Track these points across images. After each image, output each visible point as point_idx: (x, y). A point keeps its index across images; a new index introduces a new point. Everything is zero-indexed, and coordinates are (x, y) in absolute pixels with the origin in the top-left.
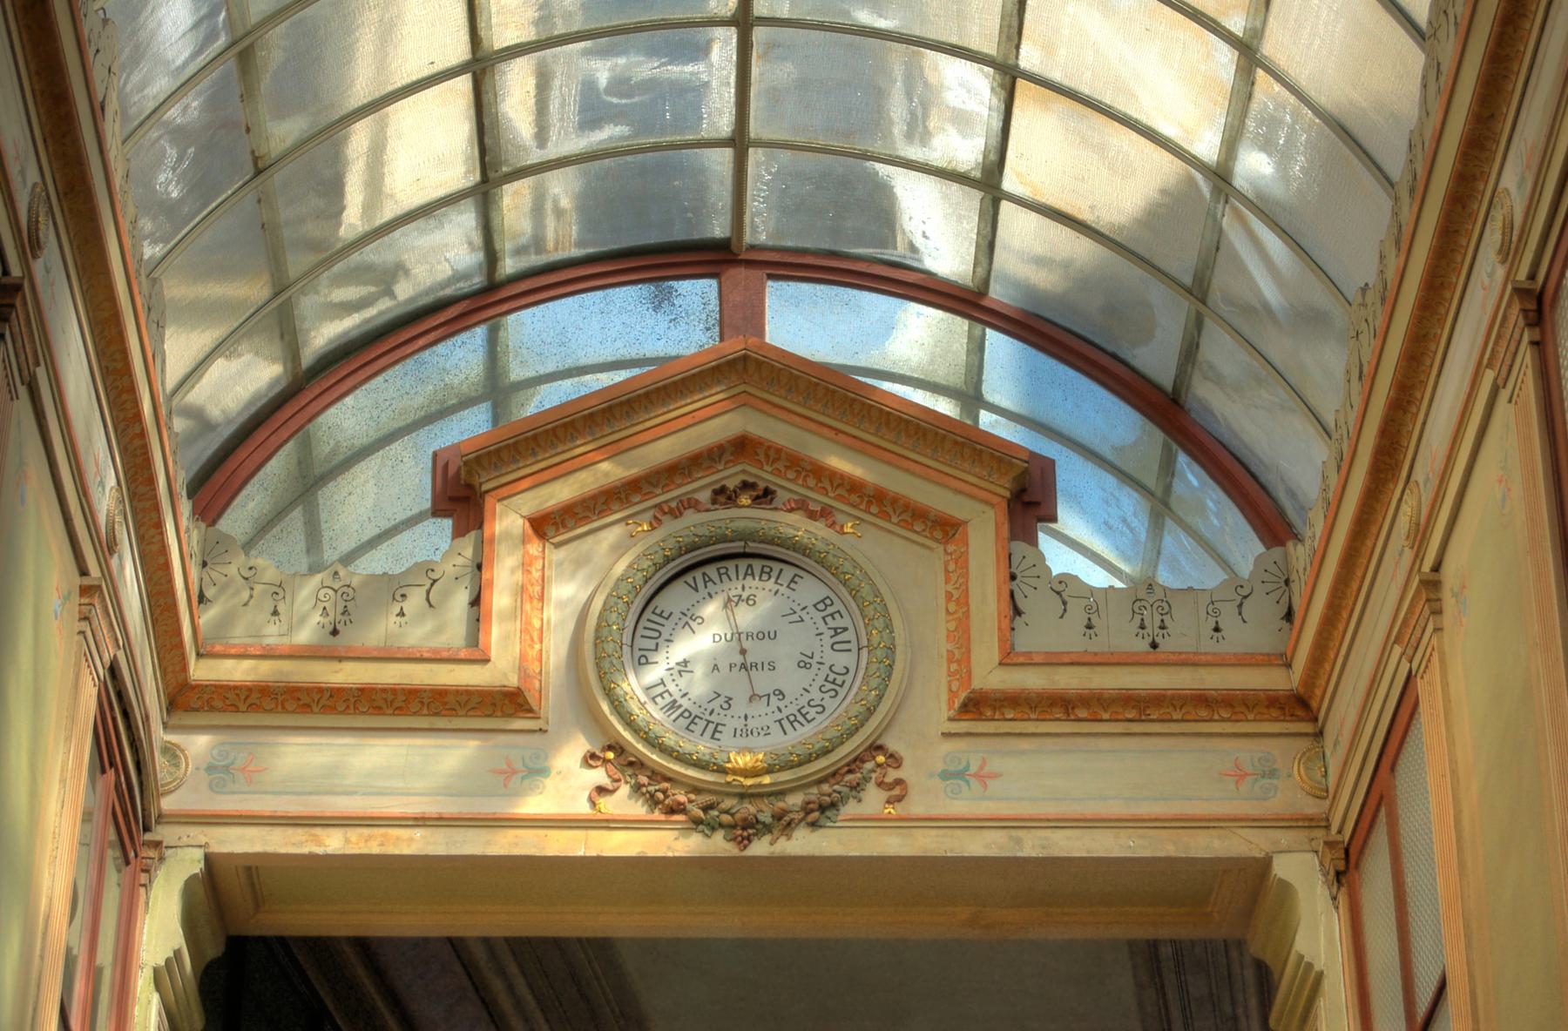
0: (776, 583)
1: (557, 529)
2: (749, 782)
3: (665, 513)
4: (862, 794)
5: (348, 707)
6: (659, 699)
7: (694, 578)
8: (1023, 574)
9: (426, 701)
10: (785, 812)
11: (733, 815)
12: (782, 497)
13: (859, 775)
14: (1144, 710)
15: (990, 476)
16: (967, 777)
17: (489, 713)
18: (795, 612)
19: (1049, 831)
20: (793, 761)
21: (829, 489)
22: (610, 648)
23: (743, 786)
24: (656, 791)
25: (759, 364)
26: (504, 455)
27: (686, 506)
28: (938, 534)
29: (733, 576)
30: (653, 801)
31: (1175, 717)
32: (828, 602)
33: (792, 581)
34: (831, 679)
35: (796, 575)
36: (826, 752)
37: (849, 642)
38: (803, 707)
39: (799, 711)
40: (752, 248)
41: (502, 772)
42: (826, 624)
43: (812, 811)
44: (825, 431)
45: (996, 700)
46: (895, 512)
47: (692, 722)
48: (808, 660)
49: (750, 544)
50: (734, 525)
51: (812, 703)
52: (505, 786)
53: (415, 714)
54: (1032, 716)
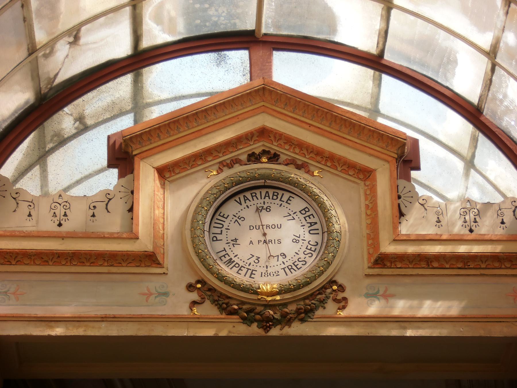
0: (280, 200)
1: (171, 174)
2: (269, 299)
3: (224, 166)
4: (326, 305)
5: (67, 262)
6: (223, 258)
7: (239, 198)
8: (404, 196)
9: (106, 259)
10: (287, 314)
11: (261, 315)
12: (283, 158)
13: (324, 295)
14: (467, 263)
15: (387, 147)
16: (378, 297)
17: (138, 265)
18: (290, 215)
19: (420, 323)
21: (306, 154)
22: (198, 232)
23: (266, 301)
24: (223, 303)
25: (271, 92)
26: (144, 137)
27: (235, 162)
28: (361, 176)
29: (259, 197)
31: (482, 267)
32: (307, 210)
33: (289, 199)
34: (309, 248)
35: (290, 197)
36: (307, 284)
37: (318, 229)
38: (296, 262)
39: (293, 264)
40: (265, 35)
42: (306, 220)
43: (301, 313)
44: (304, 125)
45: (392, 258)
46: (339, 165)
47: (240, 269)
48: (297, 239)
50: (259, 172)
51: (300, 260)
52: (147, 301)
53: (101, 265)
54: (410, 266)
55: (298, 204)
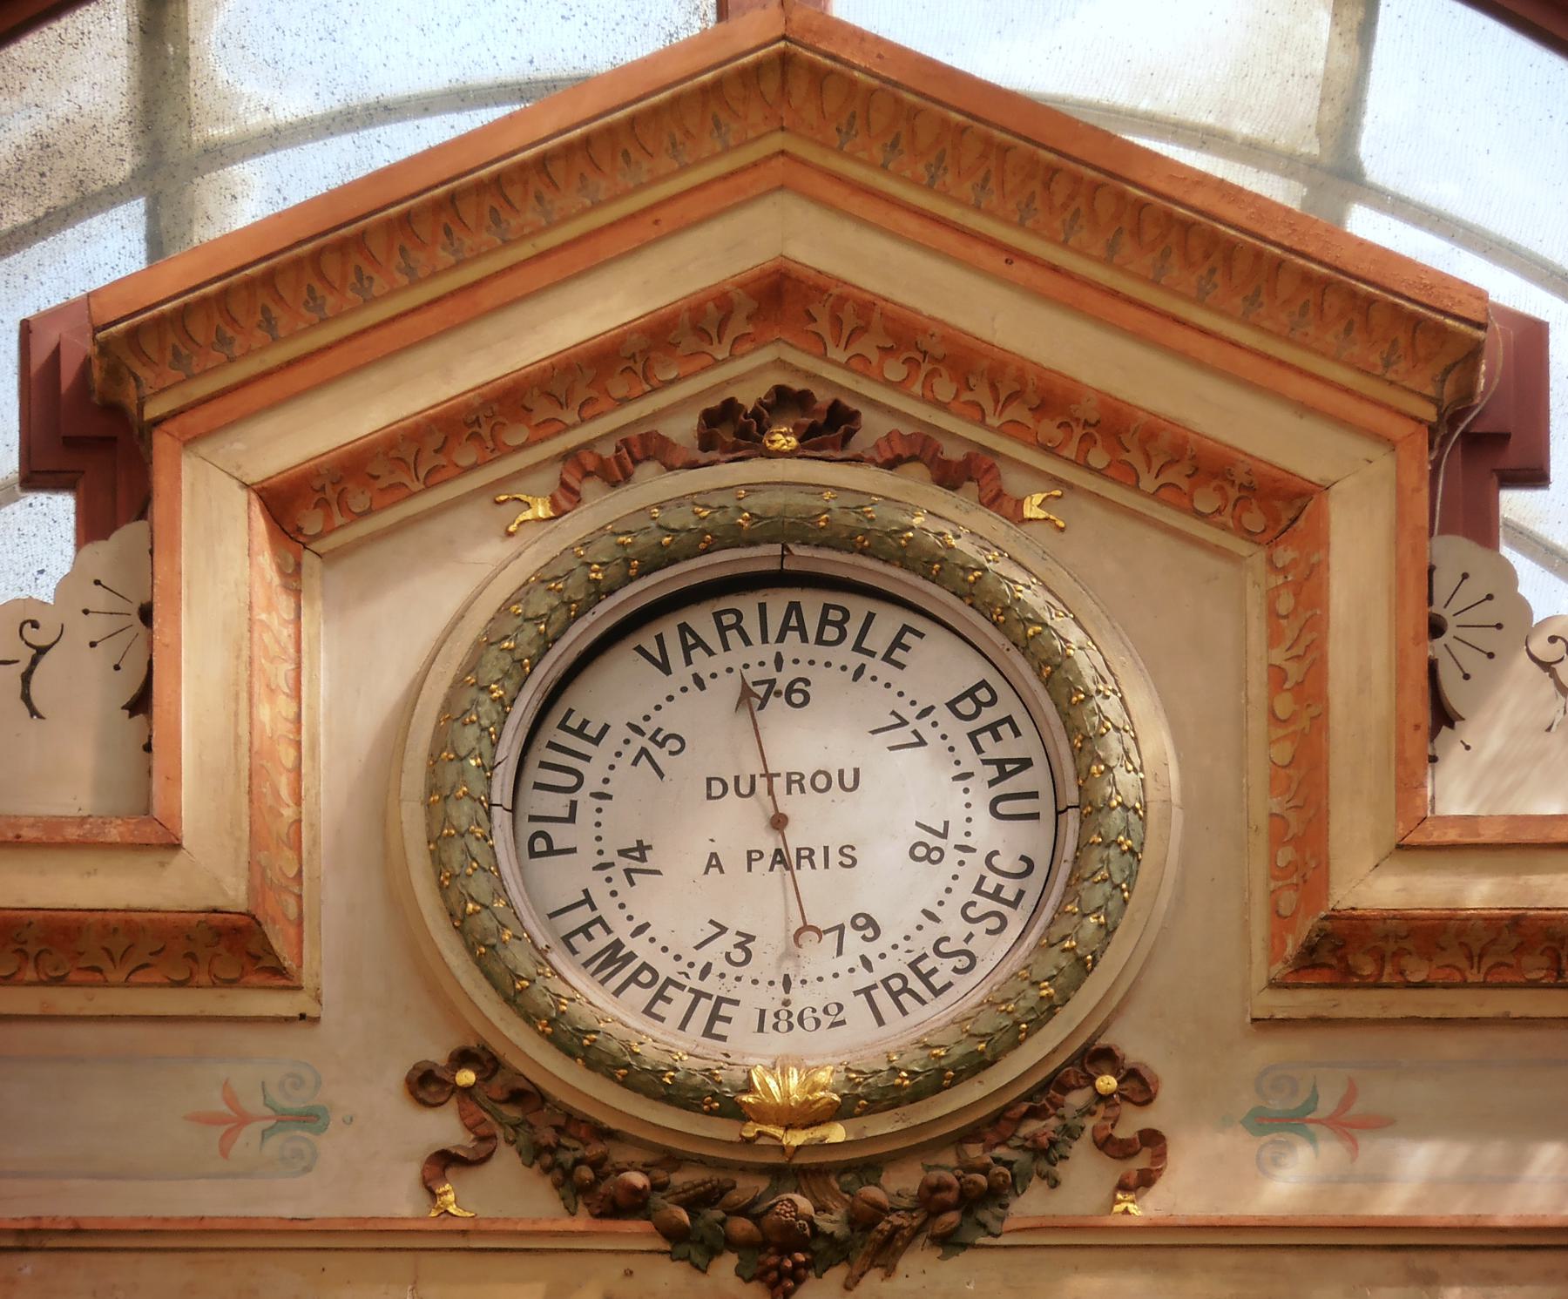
0: (858, 647)
2: (796, 1138)
6: (579, 941)
10: (880, 1211)
11: (757, 1219)
13: (1053, 1122)
17: (177, 977)
18: (904, 723)
20: (899, 1087)
21: (988, 405)
28: (1255, 520)
29: (754, 632)
32: (983, 695)
33: (897, 643)
34: (989, 887)
35: (906, 629)
36: (976, 1065)
37: (1034, 795)
38: (924, 956)
39: (913, 966)
41: (212, 1120)
42: (979, 750)
47: (660, 996)
48: (934, 841)
49: (799, 551)
50: (756, 503)
51: (944, 947)
54: (1473, 976)
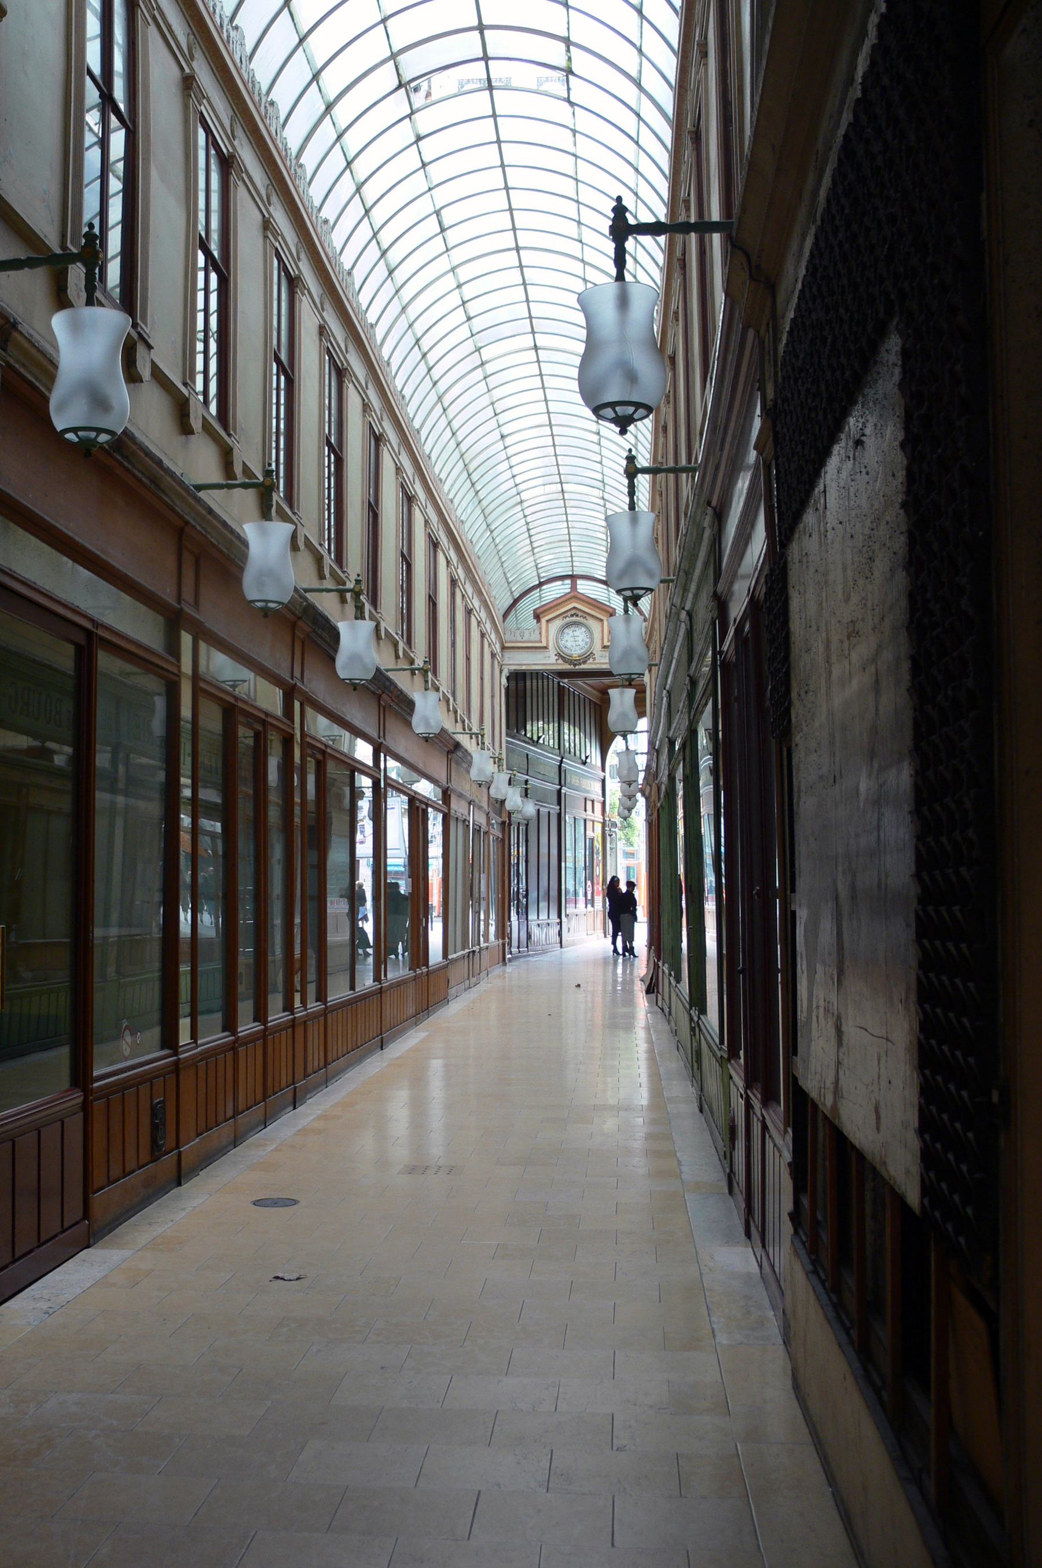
12: (580, 615)
30: (564, 661)
55: (583, 629)
